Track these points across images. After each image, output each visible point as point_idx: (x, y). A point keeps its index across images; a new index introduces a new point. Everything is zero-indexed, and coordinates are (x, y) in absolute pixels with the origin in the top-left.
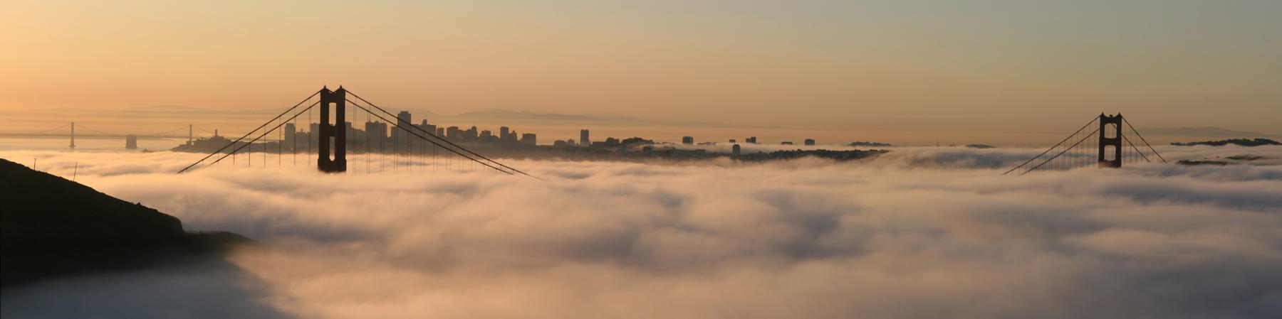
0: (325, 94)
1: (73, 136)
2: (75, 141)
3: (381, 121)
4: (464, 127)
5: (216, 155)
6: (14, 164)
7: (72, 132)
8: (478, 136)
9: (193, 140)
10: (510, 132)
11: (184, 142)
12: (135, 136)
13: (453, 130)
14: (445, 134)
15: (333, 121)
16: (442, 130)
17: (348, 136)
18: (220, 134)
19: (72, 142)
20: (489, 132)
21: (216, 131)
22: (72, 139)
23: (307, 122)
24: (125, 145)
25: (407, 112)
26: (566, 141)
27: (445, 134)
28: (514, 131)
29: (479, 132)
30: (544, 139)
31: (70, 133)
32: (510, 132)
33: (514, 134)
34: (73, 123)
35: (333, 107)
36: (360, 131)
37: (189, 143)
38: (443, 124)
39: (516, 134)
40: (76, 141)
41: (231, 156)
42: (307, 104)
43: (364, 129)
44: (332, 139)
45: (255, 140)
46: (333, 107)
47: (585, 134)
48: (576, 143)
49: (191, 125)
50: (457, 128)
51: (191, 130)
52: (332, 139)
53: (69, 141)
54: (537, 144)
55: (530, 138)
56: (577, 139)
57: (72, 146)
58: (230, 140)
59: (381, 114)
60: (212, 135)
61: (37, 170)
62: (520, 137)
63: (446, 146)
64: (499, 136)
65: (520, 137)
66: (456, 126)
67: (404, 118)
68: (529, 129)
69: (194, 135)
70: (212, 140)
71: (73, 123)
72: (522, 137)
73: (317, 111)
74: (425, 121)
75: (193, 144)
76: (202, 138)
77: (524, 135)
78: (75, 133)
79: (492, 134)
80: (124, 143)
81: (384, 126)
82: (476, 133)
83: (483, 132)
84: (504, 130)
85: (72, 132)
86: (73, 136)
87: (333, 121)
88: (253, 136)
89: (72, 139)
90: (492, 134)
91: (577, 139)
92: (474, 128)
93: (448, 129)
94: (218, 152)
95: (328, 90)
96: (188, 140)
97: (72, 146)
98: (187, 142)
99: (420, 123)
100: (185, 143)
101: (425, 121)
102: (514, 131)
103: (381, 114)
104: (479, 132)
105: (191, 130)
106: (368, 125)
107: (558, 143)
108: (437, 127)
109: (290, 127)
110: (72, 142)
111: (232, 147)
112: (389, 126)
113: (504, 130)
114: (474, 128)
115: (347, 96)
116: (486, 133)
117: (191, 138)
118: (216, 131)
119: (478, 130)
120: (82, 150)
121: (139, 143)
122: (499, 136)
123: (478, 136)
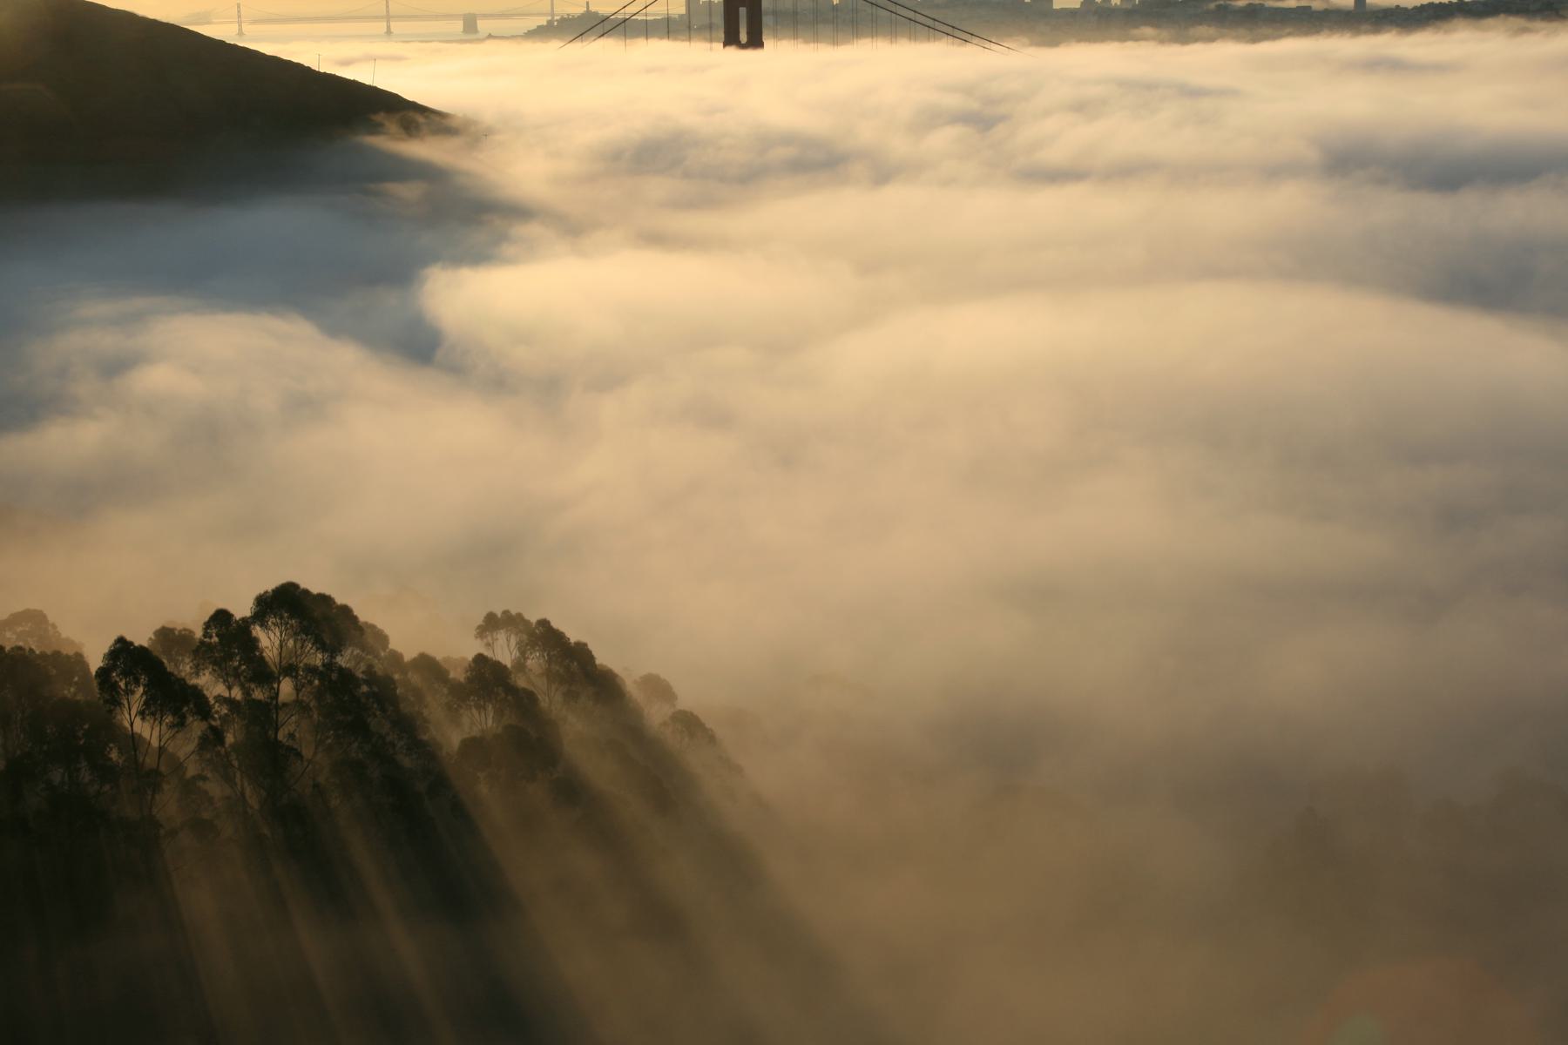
1: (388, 18)
2: (392, 24)
6: (290, 62)
7: (388, 12)
9: (556, 18)
11: (543, 21)
18: (593, 8)
19: (388, 27)
21: (588, 3)
22: (388, 21)
24: (462, 30)
31: (384, 13)
37: (550, 23)
44: (743, 11)
45: (635, 14)
52: (743, 11)
53: (384, 25)
54: (1055, 7)
57: (389, 32)
60: (582, 10)
61: (322, 71)
63: (910, 16)
69: (558, 10)
70: (582, 17)
75: (556, 24)
76: (568, 15)
78: (391, 13)
80: (459, 26)
85: (388, 12)
86: (388, 18)
89: (388, 21)
96: (550, 18)
97: (389, 32)
100: (545, 23)
110: (388, 27)
111: (599, 29)
117: (553, 14)
118: (588, 3)
121: (482, 25)
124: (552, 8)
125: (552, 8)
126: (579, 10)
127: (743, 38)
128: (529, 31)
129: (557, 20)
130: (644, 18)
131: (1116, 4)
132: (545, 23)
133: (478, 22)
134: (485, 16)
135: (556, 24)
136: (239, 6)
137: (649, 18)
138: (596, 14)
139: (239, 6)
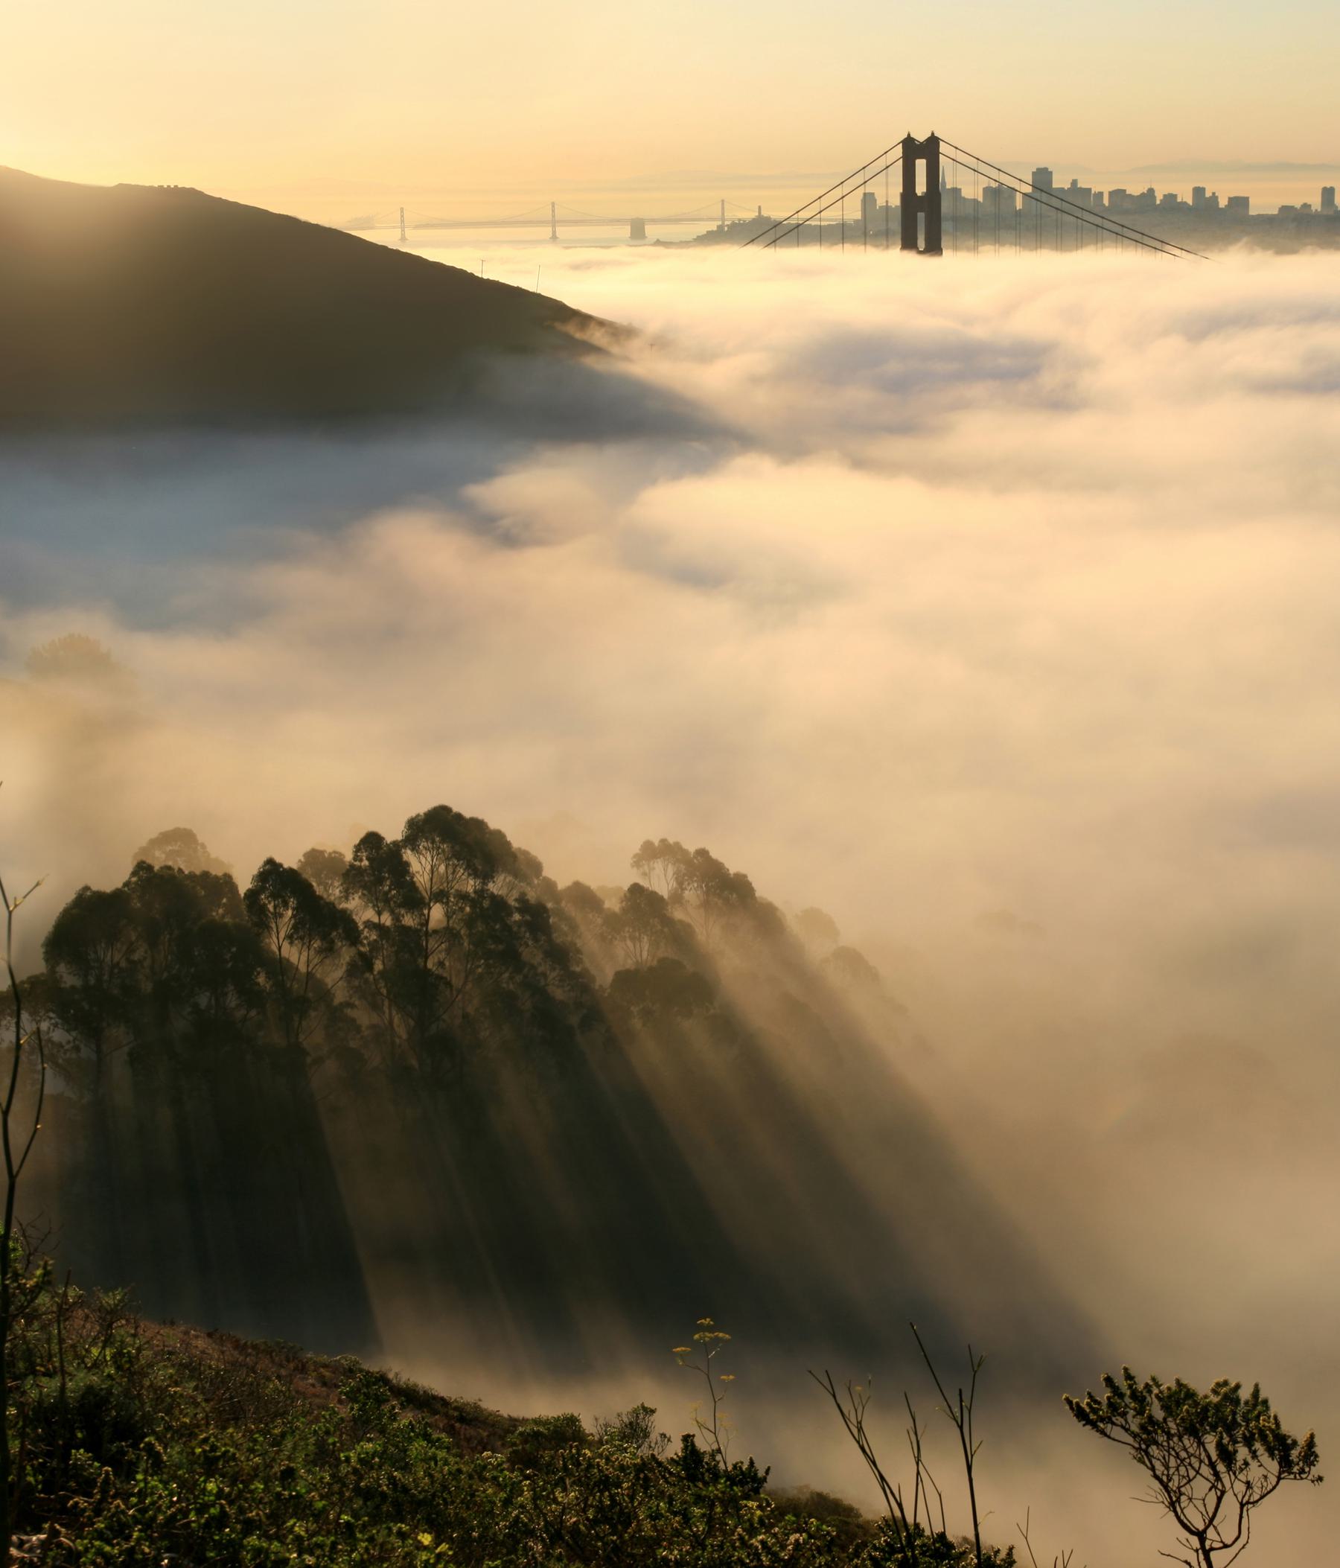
0: (909, 143)
1: (554, 223)
4: (1135, 189)
6: (453, 269)
7: (553, 216)
8: (1158, 202)
9: (727, 223)
10: (1208, 194)
11: (713, 226)
13: (1118, 194)
14: (1106, 202)
15: (921, 188)
16: (1101, 194)
17: (946, 206)
18: (765, 213)
19: (554, 232)
20: (1175, 196)
21: (760, 207)
22: (554, 226)
23: (890, 193)
25: (1046, 169)
26: (1298, 206)
27: (1106, 202)
28: (1214, 194)
30: (1264, 202)
32: (1208, 194)
33: (1214, 197)
34: (553, 204)
35: (921, 165)
36: (975, 201)
38: (1102, 185)
39: (1217, 197)
40: (561, 231)
42: (881, 163)
43: (981, 199)
44: (921, 216)
46: (921, 165)
47: (1328, 193)
48: (1313, 209)
49: (723, 201)
50: (1125, 191)
51: (723, 208)
52: (921, 216)
55: (1239, 203)
56: (1316, 203)
57: (554, 237)
60: (754, 215)
61: (485, 277)
62: (1223, 203)
64: (1190, 202)
65: (1223, 203)
67: (1042, 178)
68: (1238, 190)
71: (553, 204)
73: (898, 169)
74: (1074, 182)
75: (726, 229)
76: (739, 220)
79: (1179, 200)
80: (626, 231)
82: (1155, 197)
83: (1165, 196)
84: (1198, 192)
85: (553, 216)
86: (554, 223)
87: (921, 188)
88: (804, 215)
89: (554, 226)
90: (1179, 200)
91: (1316, 203)
92: (1151, 191)
93: (1111, 193)
95: (914, 139)
96: (720, 223)
97: (554, 237)
98: (718, 227)
99: (1067, 186)
100: (715, 229)
101: (1074, 182)
102: (1214, 194)
103: (994, 174)
105: (723, 208)
107: (1284, 209)
108: (1093, 192)
109: (868, 199)
110: (554, 232)
111: (771, 235)
113: (1198, 192)
114: (1151, 191)
115: (943, 148)
116: (1170, 198)
117: (723, 219)
118: (760, 207)
119: (1156, 194)
120: (569, 245)
121: (652, 231)
122: (1190, 202)
123: (1158, 202)
124: (723, 214)
125: (723, 214)
126: (750, 215)
127: (921, 244)
128: (698, 237)
129: (728, 225)
130: (819, 223)
131: (1316, 210)
133: (646, 226)
134: (654, 221)
135: (726, 229)
136: (402, 210)
137: (823, 223)
138: (768, 219)
139: (402, 210)
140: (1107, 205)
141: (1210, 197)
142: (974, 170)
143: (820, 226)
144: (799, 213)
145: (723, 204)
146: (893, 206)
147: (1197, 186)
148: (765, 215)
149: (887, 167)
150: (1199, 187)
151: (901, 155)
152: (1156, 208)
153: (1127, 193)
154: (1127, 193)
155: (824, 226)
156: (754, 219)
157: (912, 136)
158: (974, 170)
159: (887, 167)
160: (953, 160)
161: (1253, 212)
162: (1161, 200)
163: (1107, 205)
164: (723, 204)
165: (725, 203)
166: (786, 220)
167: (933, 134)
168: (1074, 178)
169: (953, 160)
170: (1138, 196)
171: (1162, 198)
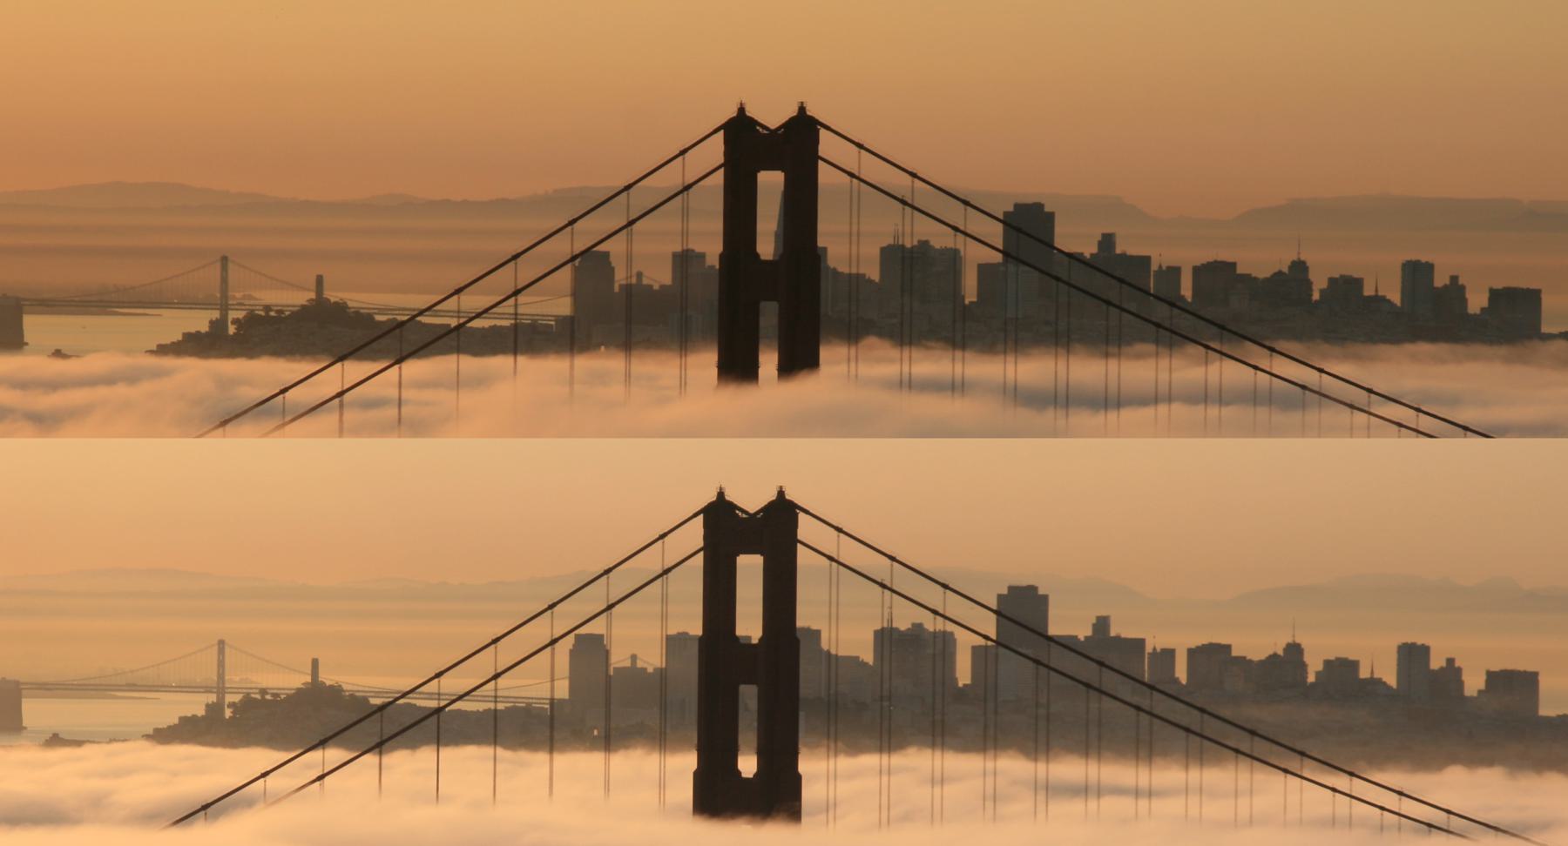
0: (719, 514)
3: (931, 624)
5: (315, 756)
8: (1311, 678)
9: (229, 698)
10: (1436, 663)
11: (195, 705)
12: (17, 683)
13: (1211, 656)
14: (1181, 672)
15: (749, 624)
16: (1169, 654)
18: (328, 678)
20: (1353, 666)
21: (315, 664)
25: (1033, 589)
27: (1181, 672)
29: (1314, 666)
32: (1436, 663)
33: (1452, 672)
35: (750, 568)
36: (855, 661)
37: (214, 710)
39: (1459, 670)
41: (370, 759)
42: (651, 562)
44: (749, 695)
46: (750, 568)
49: (221, 643)
50: (1228, 647)
51: (221, 664)
52: (749, 695)
58: (365, 699)
59: (933, 595)
60: (296, 680)
62: (1473, 683)
63: (1185, 722)
65: (1473, 683)
66: (1223, 641)
68: (1513, 653)
72: (1482, 686)
73: (691, 581)
74: (1102, 624)
75: (228, 713)
76: (263, 691)
77: (1492, 677)
79: (1364, 673)
81: (945, 642)
83: (1327, 663)
84: (1413, 655)
87: (749, 624)
88: (453, 683)
90: (1364, 673)
92: (1294, 650)
93: (1193, 653)
94: (322, 743)
96: (212, 698)
99: (1083, 631)
100: (201, 712)
101: (1102, 624)
103: (933, 595)
104: (1314, 666)
105: (221, 664)
106: (886, 638)
108: (1149, 649)
109: (590, 650)
111: (371, 728)
112: (965, 642)
113: (1413, 655)
114: (1294, 650)
115: (806, 528)
116: (1341, 670)
117: (221, 690)
119: (1307, 658)
121: (35, 712)
122: (1391, 679)
123: (1311, 678)
124: (221, 676)
125: (221, 676)
129: (232, 705)
130: (492, 706)
132: (201, 712)
134: (47, 689)
135: (228, 713)
137: (501, 706)
138: (336, 691)
140: (1184, 682)
141: (1442, 669)
142: (883, 586)
143: (496, 710)
144: (443, 679)
145: (221, 651)
146: (650, 670)
147: (1410, 640)
148: (328, 683)
149: (667, 571)
150: (1413, 645)
151: (701, 544)
152: (1307, 693)
153: (1235, 653)
154: (1235, 653)
155: (501, 710)
156: (299, 690)
157: (729, 497)
158: (883, 586)
159: (667, 571)
160: (831, 558)
161: (1547, 710)
162: (1318, 674)
163: (1184, 682)
164: (221, 651)
165: (227, 650)
166: (460, 698)
167: (781, 493)
168: (1103, 613)
169: (831, 558)
170: (1261, 662)
171: (1320, 667)
